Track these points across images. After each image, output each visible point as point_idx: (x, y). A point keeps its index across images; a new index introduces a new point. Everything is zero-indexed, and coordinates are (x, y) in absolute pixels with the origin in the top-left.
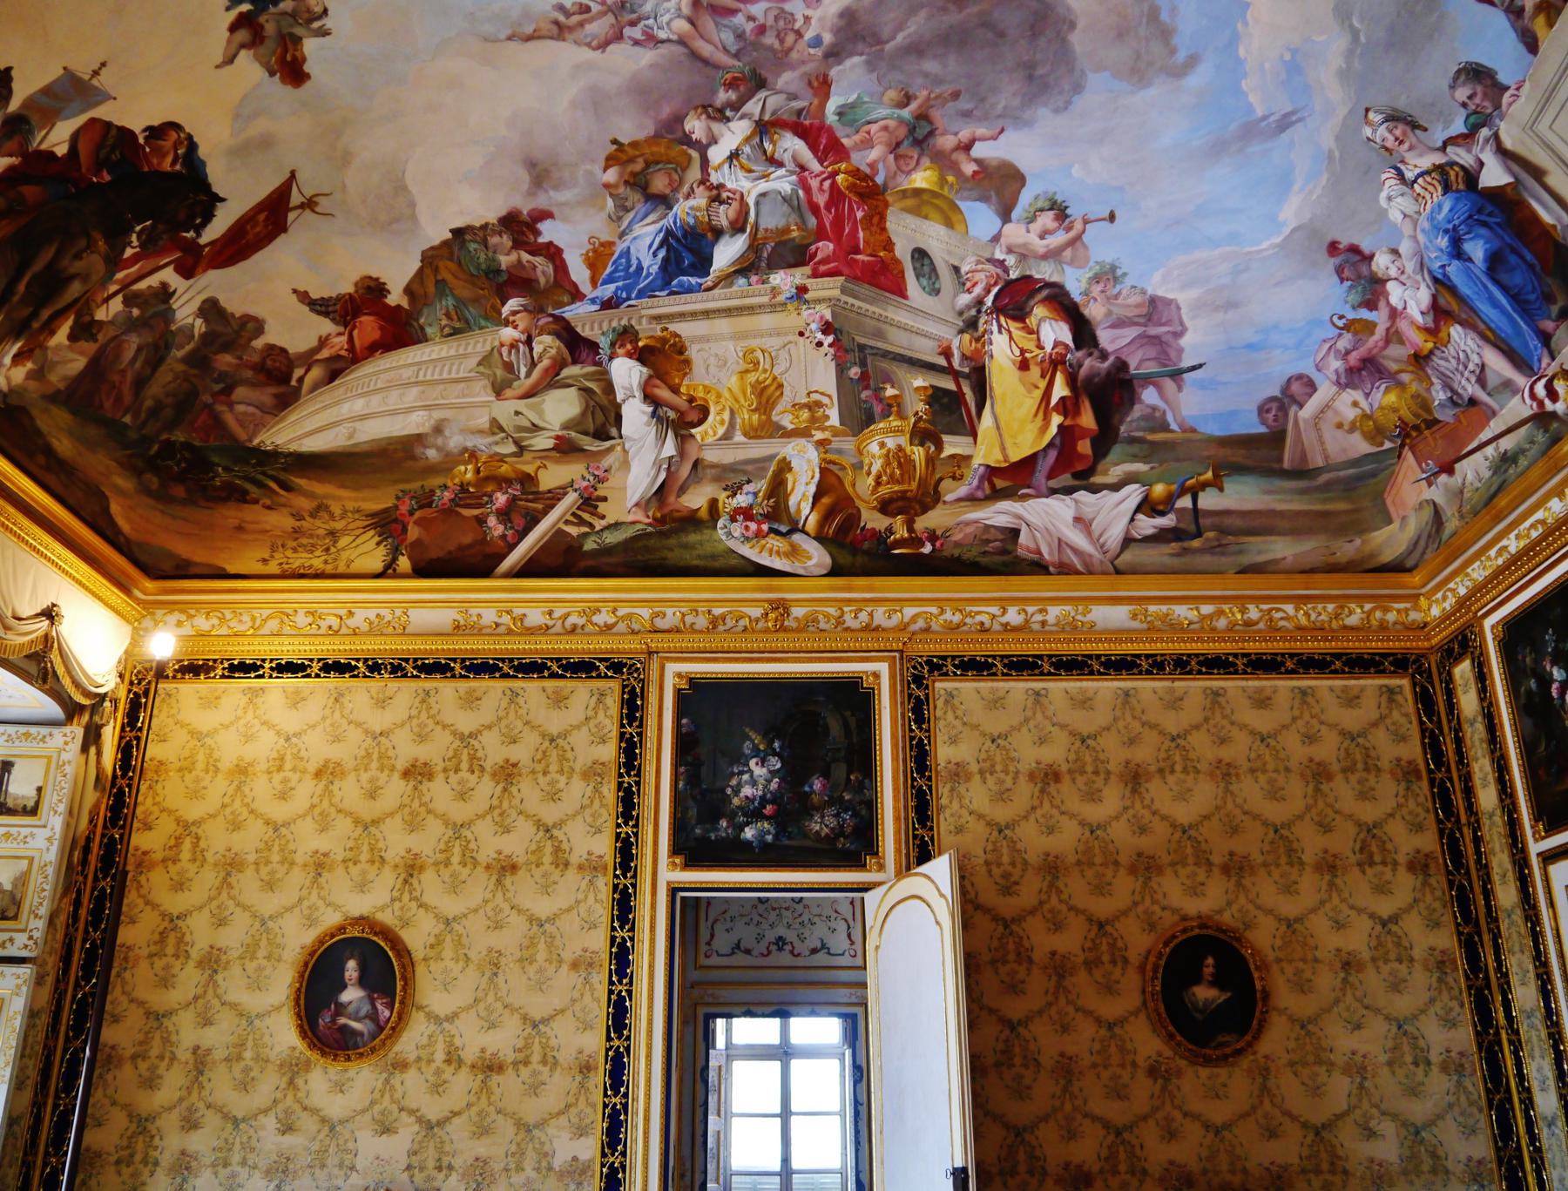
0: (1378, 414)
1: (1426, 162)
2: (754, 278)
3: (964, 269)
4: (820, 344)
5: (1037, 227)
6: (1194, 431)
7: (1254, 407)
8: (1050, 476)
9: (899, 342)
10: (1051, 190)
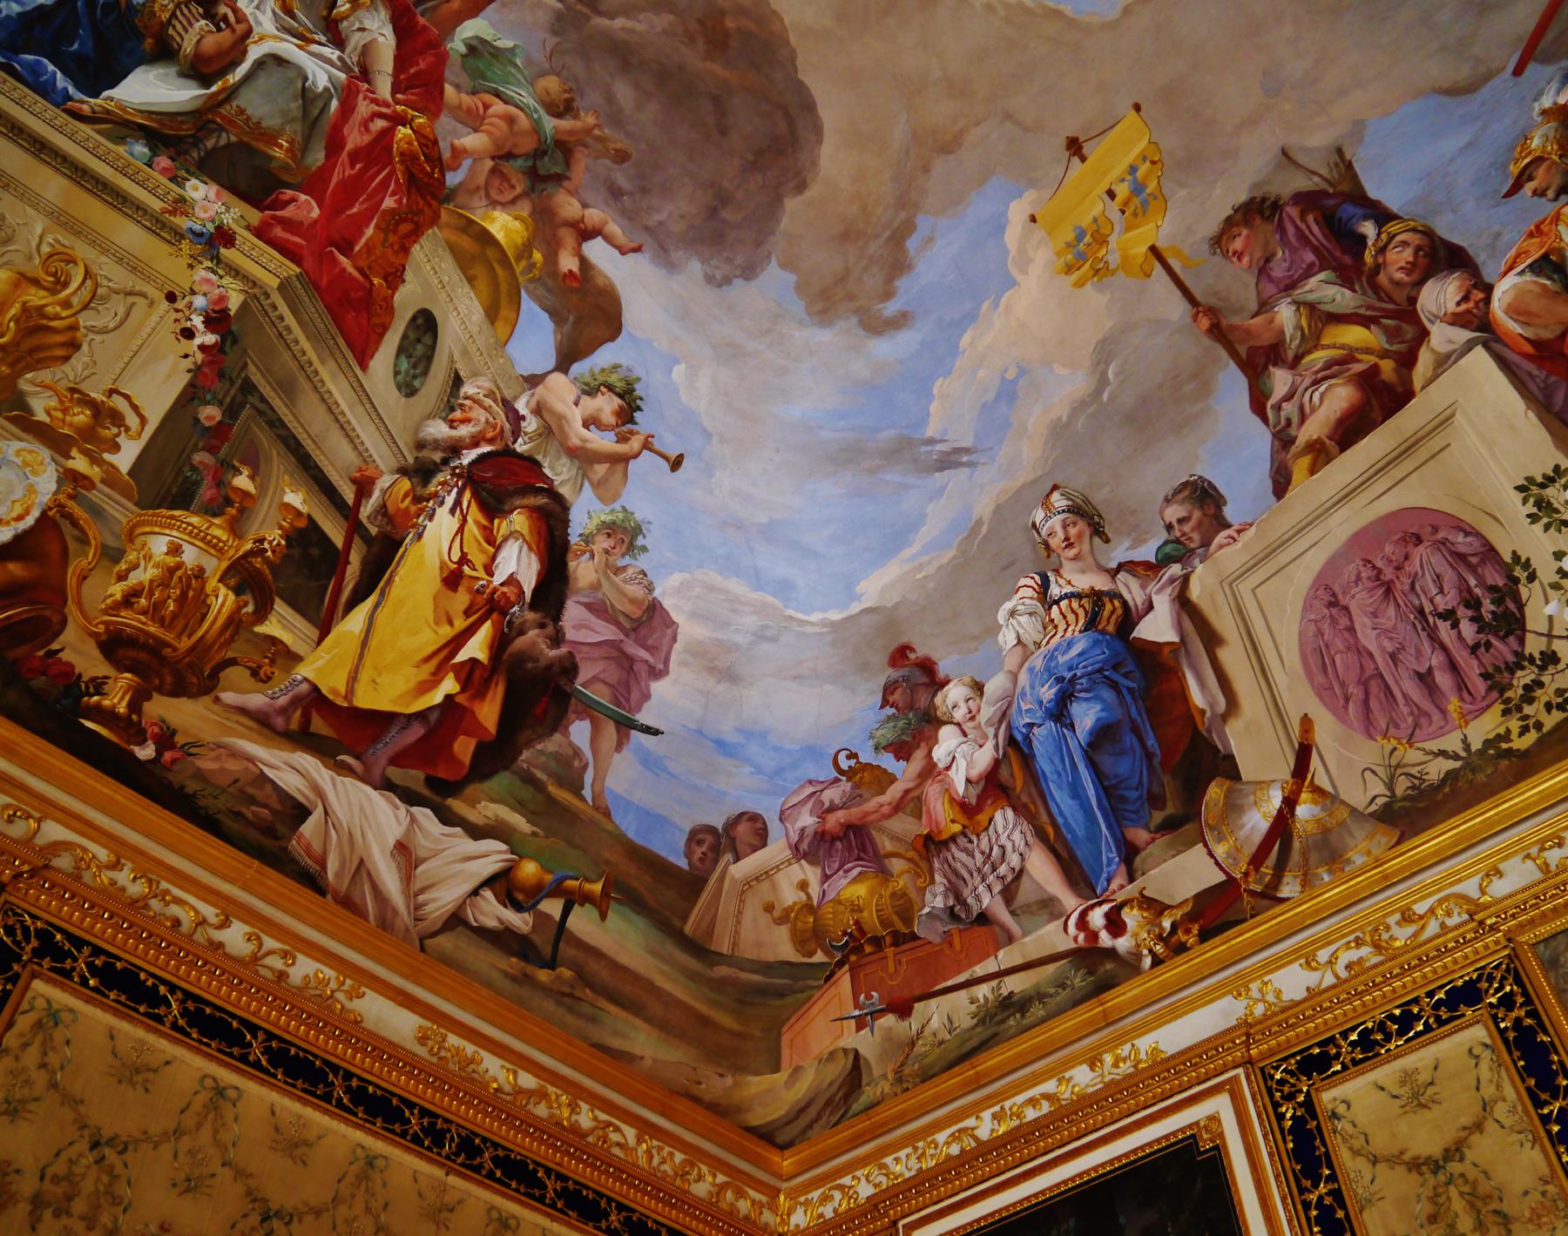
0: (827, 911)
1: (1085, 581)
2: (164, 162)
3: (468, 389)
4: (188, 334)
5: (591, 405)
6: (607, 814)
7: (687, 827)
8: (396, 760)
9: (308, 421)
10: (639, 372)
